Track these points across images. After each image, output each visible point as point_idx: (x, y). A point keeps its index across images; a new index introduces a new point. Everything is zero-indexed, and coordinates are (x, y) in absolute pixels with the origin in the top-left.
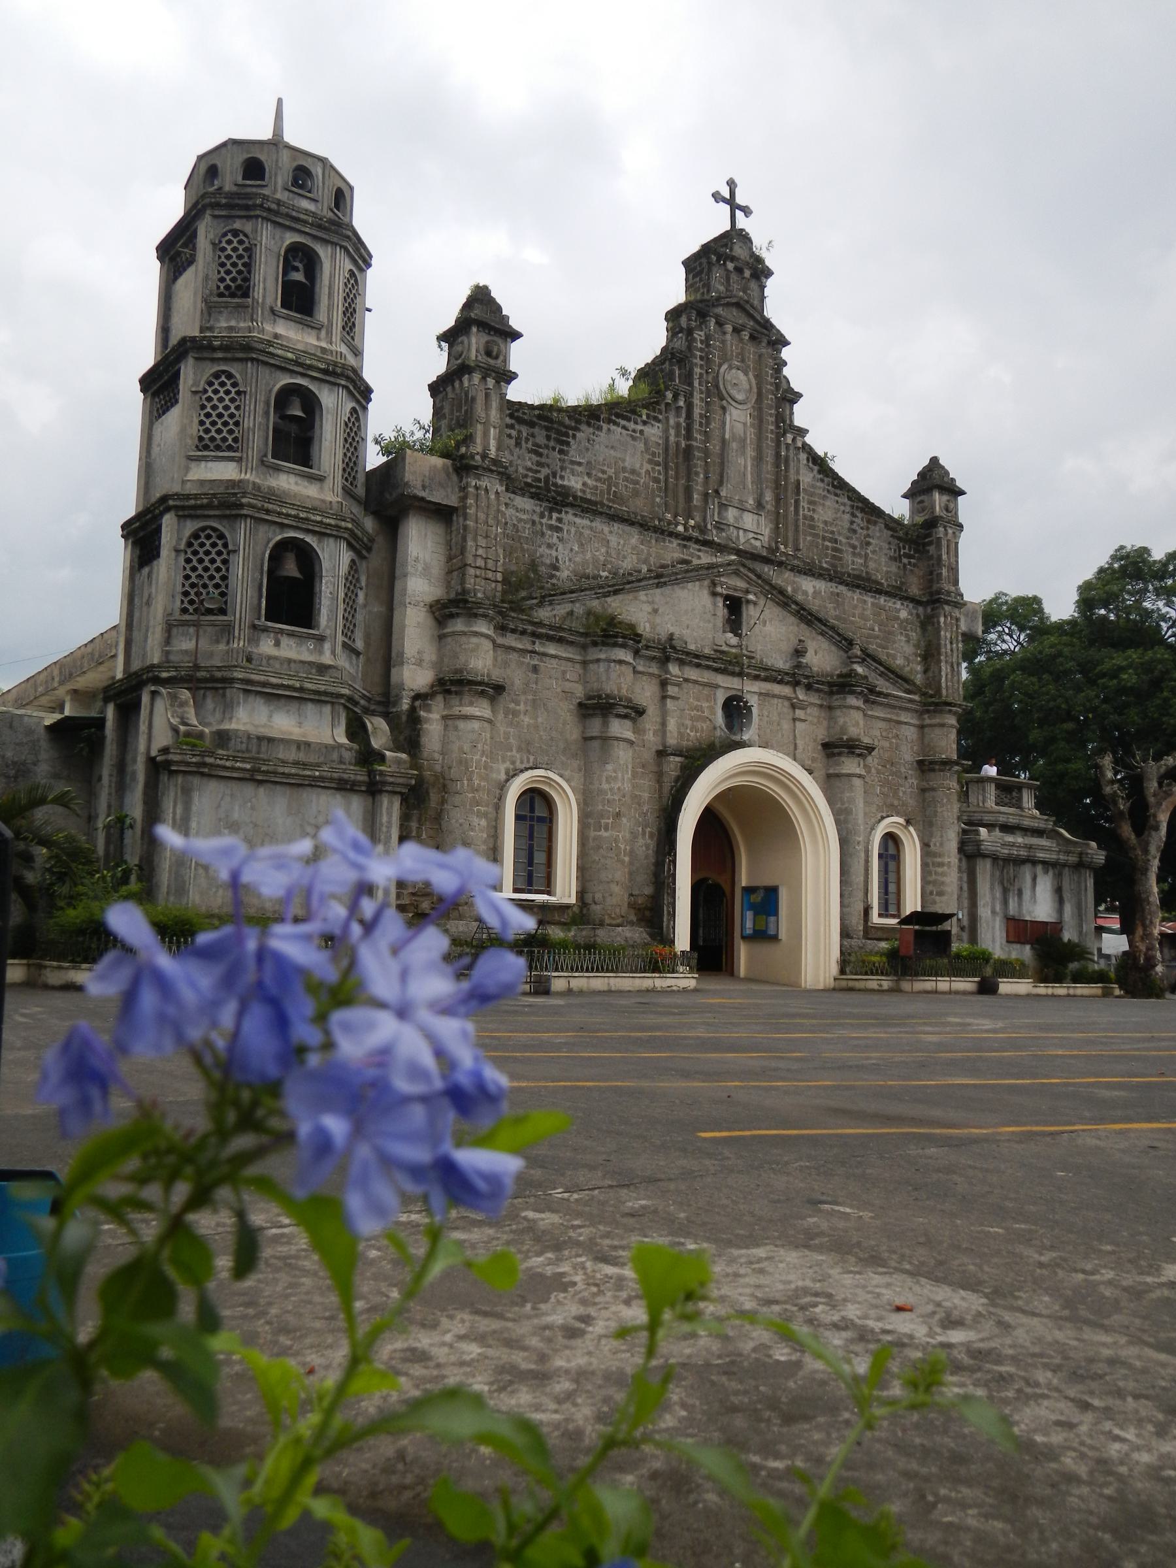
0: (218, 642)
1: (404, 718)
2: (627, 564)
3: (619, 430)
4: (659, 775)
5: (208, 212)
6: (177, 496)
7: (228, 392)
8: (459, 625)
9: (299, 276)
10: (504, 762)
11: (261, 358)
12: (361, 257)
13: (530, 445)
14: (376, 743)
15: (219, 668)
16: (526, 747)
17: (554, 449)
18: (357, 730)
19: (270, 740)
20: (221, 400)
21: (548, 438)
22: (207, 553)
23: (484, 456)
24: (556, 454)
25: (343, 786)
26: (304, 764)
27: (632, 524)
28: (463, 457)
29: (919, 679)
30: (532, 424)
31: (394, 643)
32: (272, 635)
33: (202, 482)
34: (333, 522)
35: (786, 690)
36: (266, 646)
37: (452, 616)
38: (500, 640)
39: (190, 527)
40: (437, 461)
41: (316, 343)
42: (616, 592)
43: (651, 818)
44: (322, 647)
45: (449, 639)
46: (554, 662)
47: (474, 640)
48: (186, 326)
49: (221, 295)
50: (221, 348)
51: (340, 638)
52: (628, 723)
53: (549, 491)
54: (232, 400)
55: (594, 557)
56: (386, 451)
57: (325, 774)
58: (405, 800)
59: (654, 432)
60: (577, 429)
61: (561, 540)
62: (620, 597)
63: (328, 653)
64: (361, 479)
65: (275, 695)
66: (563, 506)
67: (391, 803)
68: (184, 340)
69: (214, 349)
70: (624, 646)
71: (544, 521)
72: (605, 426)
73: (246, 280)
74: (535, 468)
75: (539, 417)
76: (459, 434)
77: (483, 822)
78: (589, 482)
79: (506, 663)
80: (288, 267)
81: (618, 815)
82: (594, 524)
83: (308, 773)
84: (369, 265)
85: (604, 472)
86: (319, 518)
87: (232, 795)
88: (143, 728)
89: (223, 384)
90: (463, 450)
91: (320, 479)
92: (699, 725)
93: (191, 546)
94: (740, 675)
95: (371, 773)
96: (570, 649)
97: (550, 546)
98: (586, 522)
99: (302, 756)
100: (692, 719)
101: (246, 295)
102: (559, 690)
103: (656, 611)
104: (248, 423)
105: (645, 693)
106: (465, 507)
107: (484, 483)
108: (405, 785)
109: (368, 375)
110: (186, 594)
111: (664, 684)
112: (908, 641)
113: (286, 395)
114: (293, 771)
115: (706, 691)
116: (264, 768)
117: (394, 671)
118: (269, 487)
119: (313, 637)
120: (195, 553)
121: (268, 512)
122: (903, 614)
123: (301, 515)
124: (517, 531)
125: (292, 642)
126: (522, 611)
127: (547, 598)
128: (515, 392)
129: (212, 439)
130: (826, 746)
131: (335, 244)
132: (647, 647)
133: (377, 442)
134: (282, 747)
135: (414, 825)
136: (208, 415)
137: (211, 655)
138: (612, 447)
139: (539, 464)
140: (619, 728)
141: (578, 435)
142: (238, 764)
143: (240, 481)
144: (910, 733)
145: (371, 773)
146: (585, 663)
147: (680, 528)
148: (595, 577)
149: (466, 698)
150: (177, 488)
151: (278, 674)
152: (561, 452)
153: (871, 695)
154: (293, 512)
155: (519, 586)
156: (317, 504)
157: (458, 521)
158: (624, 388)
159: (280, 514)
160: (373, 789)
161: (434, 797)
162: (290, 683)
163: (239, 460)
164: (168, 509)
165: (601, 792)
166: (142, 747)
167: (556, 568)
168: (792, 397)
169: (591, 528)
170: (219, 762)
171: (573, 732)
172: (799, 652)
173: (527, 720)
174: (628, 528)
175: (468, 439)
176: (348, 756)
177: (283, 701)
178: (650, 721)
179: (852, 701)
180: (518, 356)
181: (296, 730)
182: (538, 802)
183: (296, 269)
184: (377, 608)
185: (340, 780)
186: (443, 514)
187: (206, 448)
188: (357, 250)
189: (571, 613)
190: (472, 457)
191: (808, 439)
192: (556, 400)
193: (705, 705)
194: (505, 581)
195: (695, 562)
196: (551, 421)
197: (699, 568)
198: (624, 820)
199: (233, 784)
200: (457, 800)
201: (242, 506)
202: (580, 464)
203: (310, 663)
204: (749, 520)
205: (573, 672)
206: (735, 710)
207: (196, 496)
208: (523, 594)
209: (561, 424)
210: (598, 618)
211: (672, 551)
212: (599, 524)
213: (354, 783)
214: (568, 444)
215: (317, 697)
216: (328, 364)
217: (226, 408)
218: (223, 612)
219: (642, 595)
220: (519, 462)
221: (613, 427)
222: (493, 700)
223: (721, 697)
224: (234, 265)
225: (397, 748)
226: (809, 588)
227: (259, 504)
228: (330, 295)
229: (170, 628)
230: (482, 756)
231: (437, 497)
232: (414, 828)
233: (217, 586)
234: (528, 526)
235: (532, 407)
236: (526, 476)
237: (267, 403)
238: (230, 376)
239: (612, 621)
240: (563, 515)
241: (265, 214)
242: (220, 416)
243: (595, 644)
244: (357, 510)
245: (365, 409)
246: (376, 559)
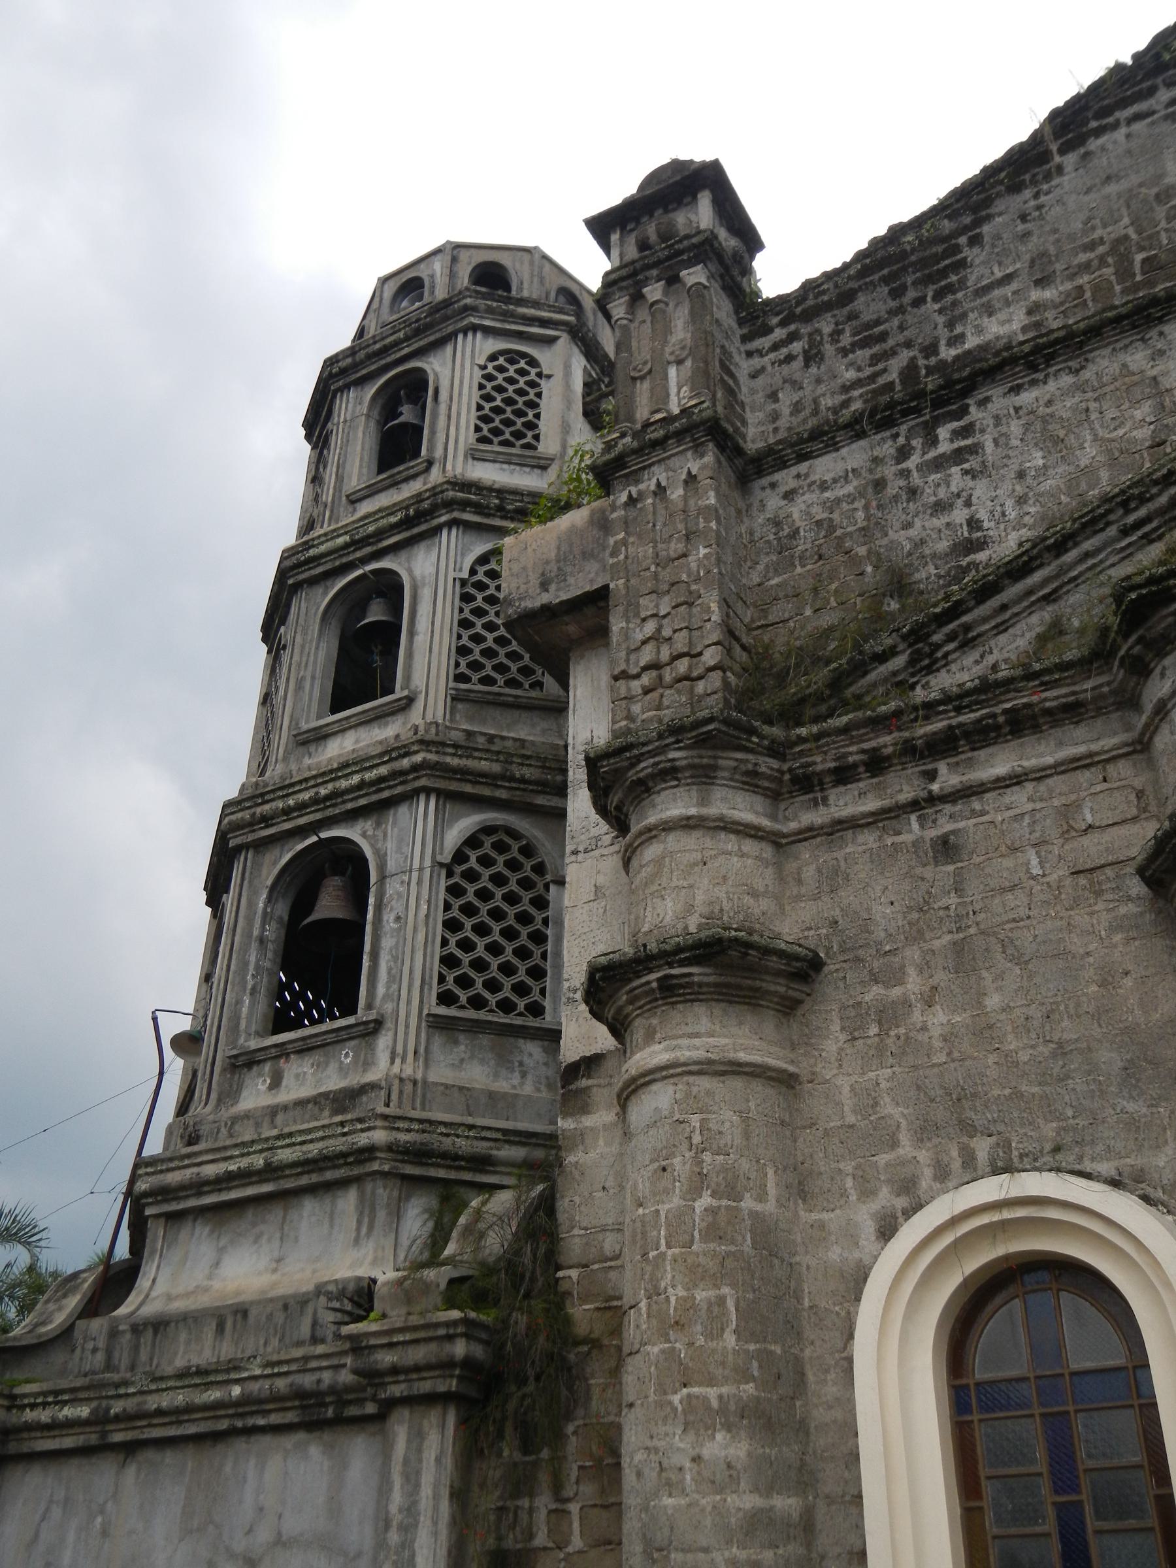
3: (1123, 130)
10: (867, 1193)
11: (301, 577)
13: (846, 340)
17: (919, 302)
21: (896, 293)
24: (932, 306)
26: (201, 1372)
32: (267, 1067)
34: (383, 770)
44: (372, 1048)
46: (1019, 798)
57: (254, 1387)
60: (978, 223)
66: (966, 393)
67: (417, 1436)
71: (912, 463)
72: (1070, 160)
74: (868, 371)
79: (836, 871)
82: (1087, 374)
83: (214, 1395)
85: (1091, 246)
86: (356, 779)
87: (67, 1502)
96: (1080, 732)
97: (940, 507)
98: (1067, 380)
102: (1063, 871)
108: (446, 1365)
114: (180, 1398)
116: (117, 1407)
119: (340, 1038)
121: (266, 820)
123: (323, 791)
124: (832, 528)
134: (183, 1336)
138: (1108, 179)
141: (986, 229)
142: (67, 1412)
151: (220, 1153)
152: (938, 297)
154: (306, 796)
159: (287, 812)
162: (243, 1163)
169: (1081, 388)
170: (29, 1415)
173: (938, 1018)
177: (250, 1214)
189: (1056, 629)
196: (904, 255)
199: (72, 1470)
202: (1008, 279)
203: (316, 1101)
214: (962, 264)
215: (315, 1178)
216: (407, 508)
220: (822, 388)
221: (1093, 144)
227: (246, 815)
230: (694, 1192)
232: (541, 1516)
234: (859, 504)
236: (845, 404)
240: (975, 413)
241: (341, 383)
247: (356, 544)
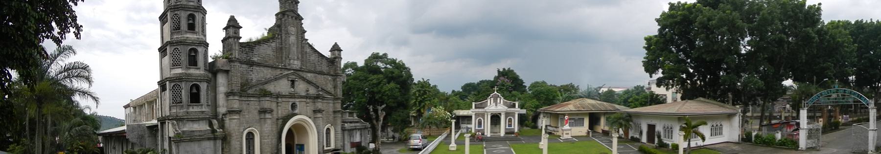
0: (181, 110)
1: (221, 120)
2: (268, 77)
4: (277, 124)
5: (170, 10)
6: (169, 78)
7: (177, 53)
8: (231, 98)
9: (191, 22)
12: (204, 12)
14: (215, 127)
15: (182, 116)
16: (247, 122)
18: (211, 125)
19: (193, 131)
20: (176, 54)
22: (177, 90)
23: (235, 58)
25: (209, 139)
27: (269, 67)
28: (230, 58)
30: (245, 47)
31: (217, 102)
33: (174, 74)
36: (191, 110)
37: (230, 95)
38: (240, 99)
39: (173, 84)
40: (224, 60)
41: (196, 37)
42: (266, 84)
43: (276, 134)
45: (229, 101)
47: (235, 101)
48: (167, 38)
49: (174, 30)
50: (176, 43)
51: (206, 104)
52: (270, 114)
53: (249, 62)
54: (179, 54)
55: (261, 76)
56: (213, 59)
58: (222, 140)
61: (253, 73)
62: (267, 84)
63: (204, 108)
64: (208, 65)
65: (193, 120)
68: (167, 42)
69: (174, 43)
70: (268, 97)
73: (179, 25)
75: (247, 45)
76: (229, 53)
77: (239, 143)
78: (259, 58)
80: (189, 20)
81: (268, 136)
84: (206, 14)
88: (167, 130)
89: (176, 51)
90: (230, 57)
91: (199, 68)
92: (286, 111)
93: (173, 89)
94: (295, 98)
95: (214, 135)
97: (250, 75)
99: (200, 134)
100: (285, 110)
101: (179, 29)
103: (275, 86)
104: (183, 59)
105: (273, 106)
106: (231, 70)
107: (235, 64)
109: (207, 41)
110: (173, 99)
111: (278, 103)
113: (191, 50)
115: (287, 103)
117: (218, 109)
118: (189, 73)
119: (200, 105)
120: (174, 90)
121: (189, 79)
125: (196, 107)
126: (245, 91)
127: (250, 88)
128: (241, 41)
129: (175, 64)
131: (199, 12)
132: (274, 95)
133: (211, 57)
135: (225, 145)
136: (174, 58)
137: (180, 113)
139: (247, 56)
140: (268, 116)
143: (182, 73)
145: (214, 135)
146: (260, 101)
147: (280, 66)
148: (262, 80)
149: (234, 114)
150: (169, 76)
151: (194, 116)
152: (252, 52)
155: (244, 85)
156: (200, 75)
157: (230, 73)
158: (266, 35)
160: (215, 139)
161: (228, 138)
163: (181, 68)
164: (167, 81)
165: (265, 131)
166: (167, 134)
167: (252, 80)
171: (257, 118)
173: (247, 116)
174: (268, 68)
175: (231, 54)
176: (210, 132)
178: (275, 113)
180: (242, 33)
181: (198, 127)
182: (250, 135)
183: (191, 20)
184: (213, 94)
185: (209, 138)
186: (227, 72)
187: (174, 66)
188: (203, 11)
189: (256, 90)
190: (232, 58)
192: (250, 40)
193: (287, 106)
194: (241, 85)
195: (284, 74)
197: (285, 75)
198: (270, 137)
200: (233, 138)
201: (183, 79)
203: (200, 111)
205: (257, 103)
206: (294, 106)
207: (173, 78)
208: (245, 87)
209: (252, 46)
210: (262, 90)
211: (278, 72)
212: (261, 68)
213: (211, 138)
214: (253, 50)
217: (178, 56)
218: (181, 103)
219: (272, 83)
222: (239, 114)
223: (290, 104)
224: (176, 22)
225: (220, 128)
228: (198, 24)
229: (170, 107)
231: (225, 68)
233: (179, 97)
235: (245, 43)
237: (186, 53)
238: (178, 49)
239: (265, 90)
242: (176, 58)
243: (262, 97)
244: (207, 73)
245: (208, 49)
246: (212, 83)
247: (193, 43)
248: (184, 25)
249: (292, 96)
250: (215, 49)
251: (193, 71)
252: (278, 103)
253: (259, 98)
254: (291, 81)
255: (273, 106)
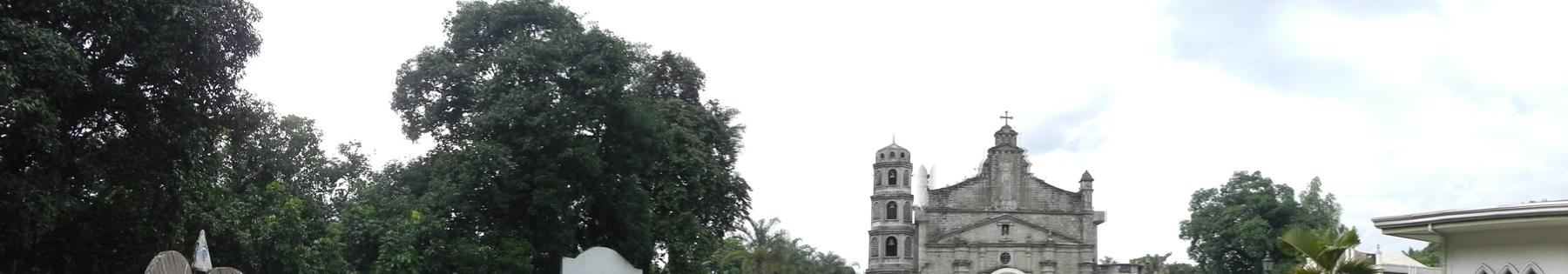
29: (1079, 238)
35: (1023, 249)
59: (976, 186)
80: (890, 175)
105: (973, 257)
112: (1075, 226)
122: (1073, 219)
130: (1041, 263)
144: (1077, 255)
153: (1056, 246)
168: (1027, 165)
172: (1029, 237)
179: (1048, 249)
191: (1035, 175)
204: (1010, 203)
206: (1005, 258)
211: (984, 217)
223: (1000, 254)
226: (1034, 218)
248: (885, 180)
249: (1002, 244)
250: (919, 199)
251: (891, 224)
252: (980, 253)
253: (953, 248)
254: (1003, 226)
255: (973, 257)
